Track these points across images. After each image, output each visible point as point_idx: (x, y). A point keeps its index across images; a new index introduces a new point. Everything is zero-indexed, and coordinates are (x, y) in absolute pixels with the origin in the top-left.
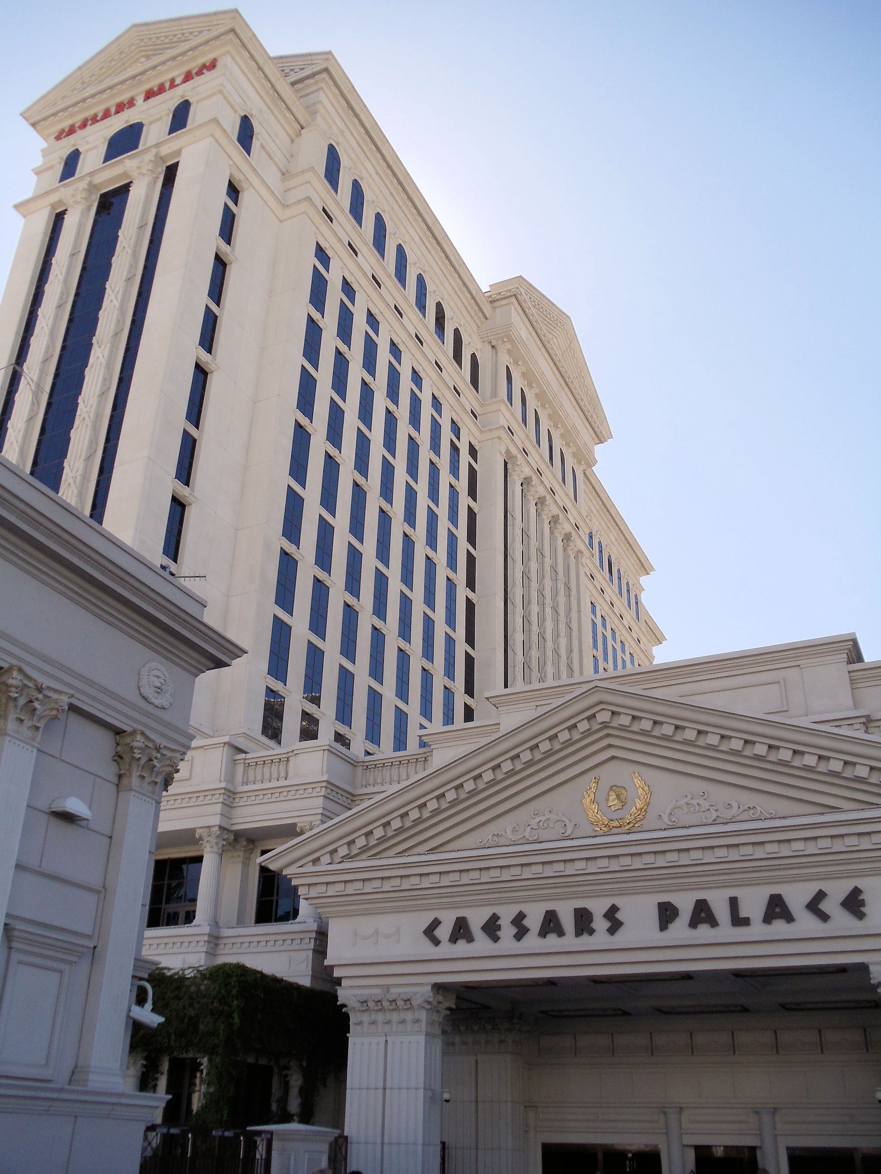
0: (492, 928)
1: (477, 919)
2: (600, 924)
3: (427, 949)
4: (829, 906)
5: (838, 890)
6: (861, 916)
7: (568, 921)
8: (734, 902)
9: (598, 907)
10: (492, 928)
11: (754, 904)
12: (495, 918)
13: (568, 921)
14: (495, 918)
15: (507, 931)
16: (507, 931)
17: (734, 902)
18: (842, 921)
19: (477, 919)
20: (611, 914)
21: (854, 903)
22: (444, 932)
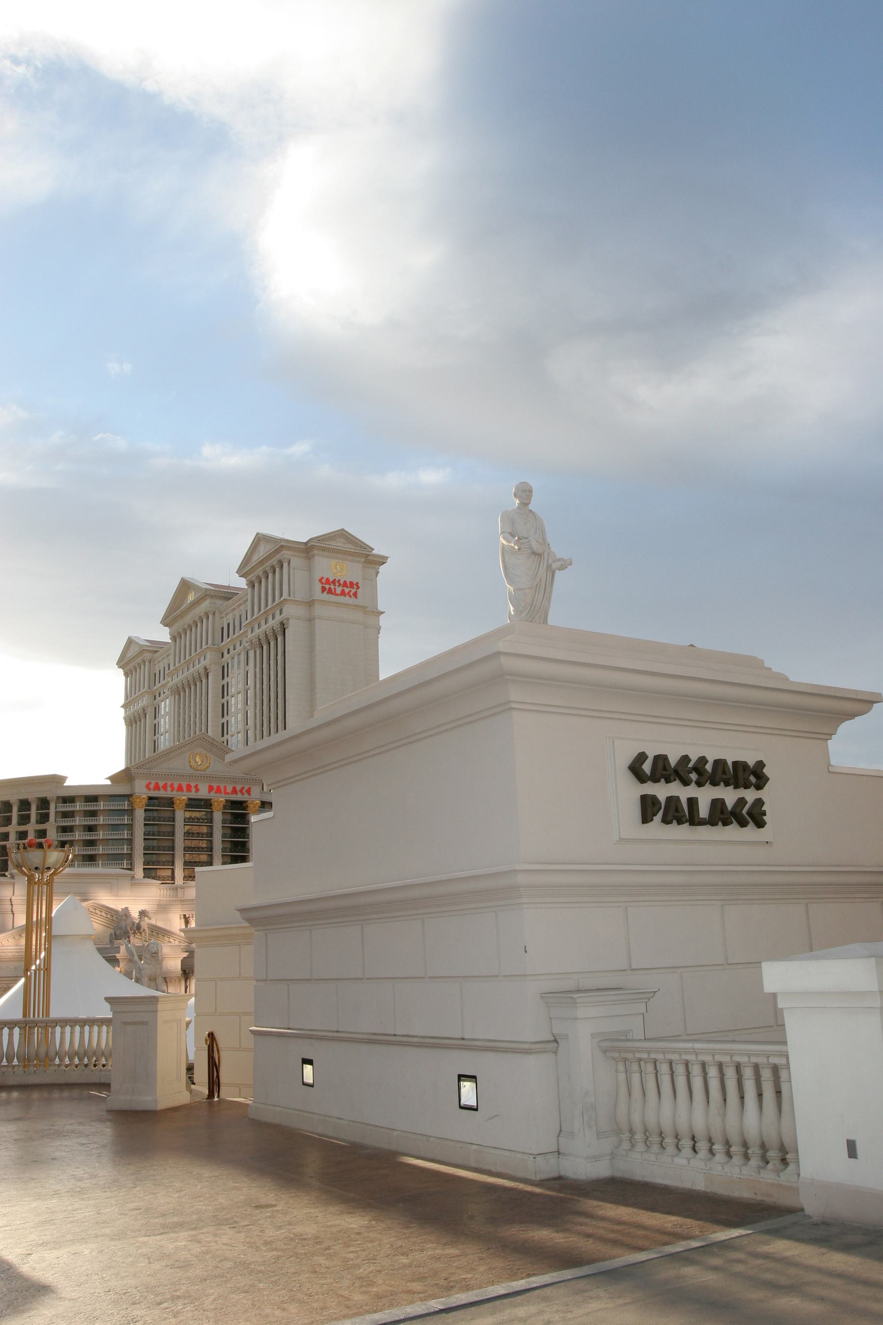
0: (165, 787)
1: (161, 784)
2: (193, 789)
3: (145, 790)
4: (244, 791)
5: (246, 788)
6: (249, 794)
7: (185, 788)
8: (225, 788)
9: (193, 785)
10: (165, 787)
11: (229, 789)
12: (166, 784)
13: (185, 788)
14: (166, 784)
15: (169, 789)
16: (169, 789)
17: (225, 788)
18: (246, 796)
19: (161, 784)
20: (196, 786)
21: (249, 791)
22: (152, 786)
